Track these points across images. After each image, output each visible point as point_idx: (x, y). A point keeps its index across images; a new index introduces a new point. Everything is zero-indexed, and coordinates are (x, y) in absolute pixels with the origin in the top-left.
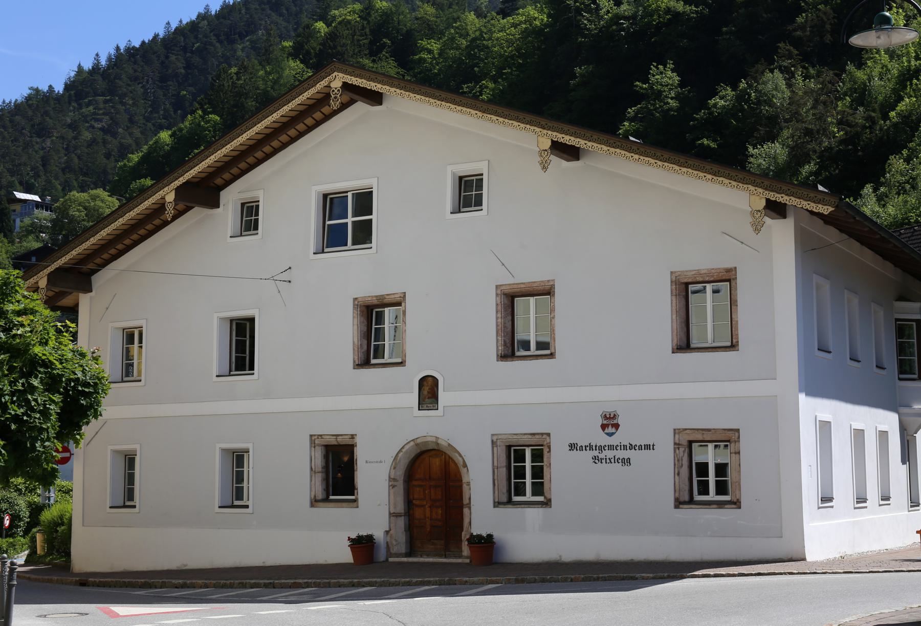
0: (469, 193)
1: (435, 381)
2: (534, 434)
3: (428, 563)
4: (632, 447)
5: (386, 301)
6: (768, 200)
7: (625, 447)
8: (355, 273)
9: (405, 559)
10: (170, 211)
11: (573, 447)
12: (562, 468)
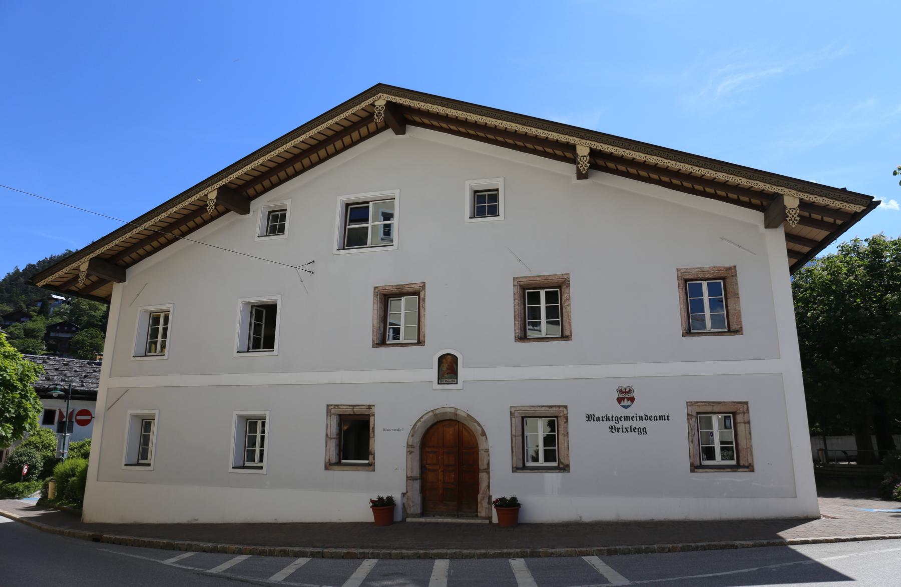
0: (485, 203)
1: (455, 359)
2: (551, 407)
3: (446, 524)
4: (647, 418)
5: (405, 290)
6: (801, 200)
7: (641, 418)
8: (376, 266)
9: (422, 520)
10: (211, 210)
11: (590, 418)
12: (579, 438)
